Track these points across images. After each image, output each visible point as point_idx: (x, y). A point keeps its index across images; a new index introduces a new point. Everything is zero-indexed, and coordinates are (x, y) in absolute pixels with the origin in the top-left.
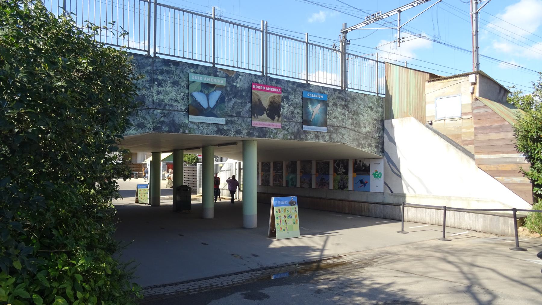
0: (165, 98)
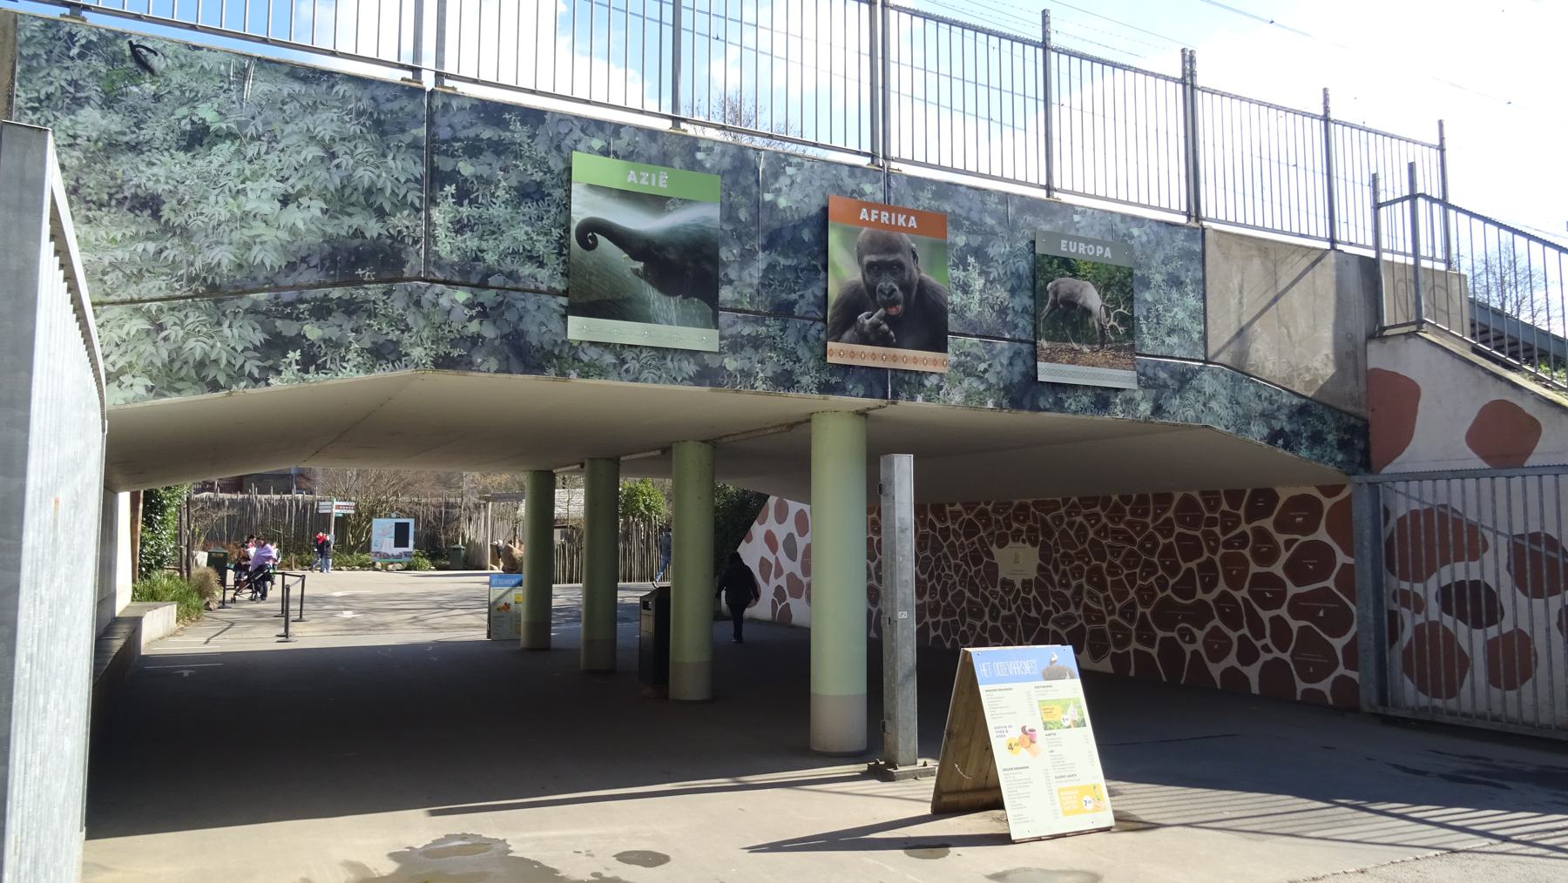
0: (484, 245)
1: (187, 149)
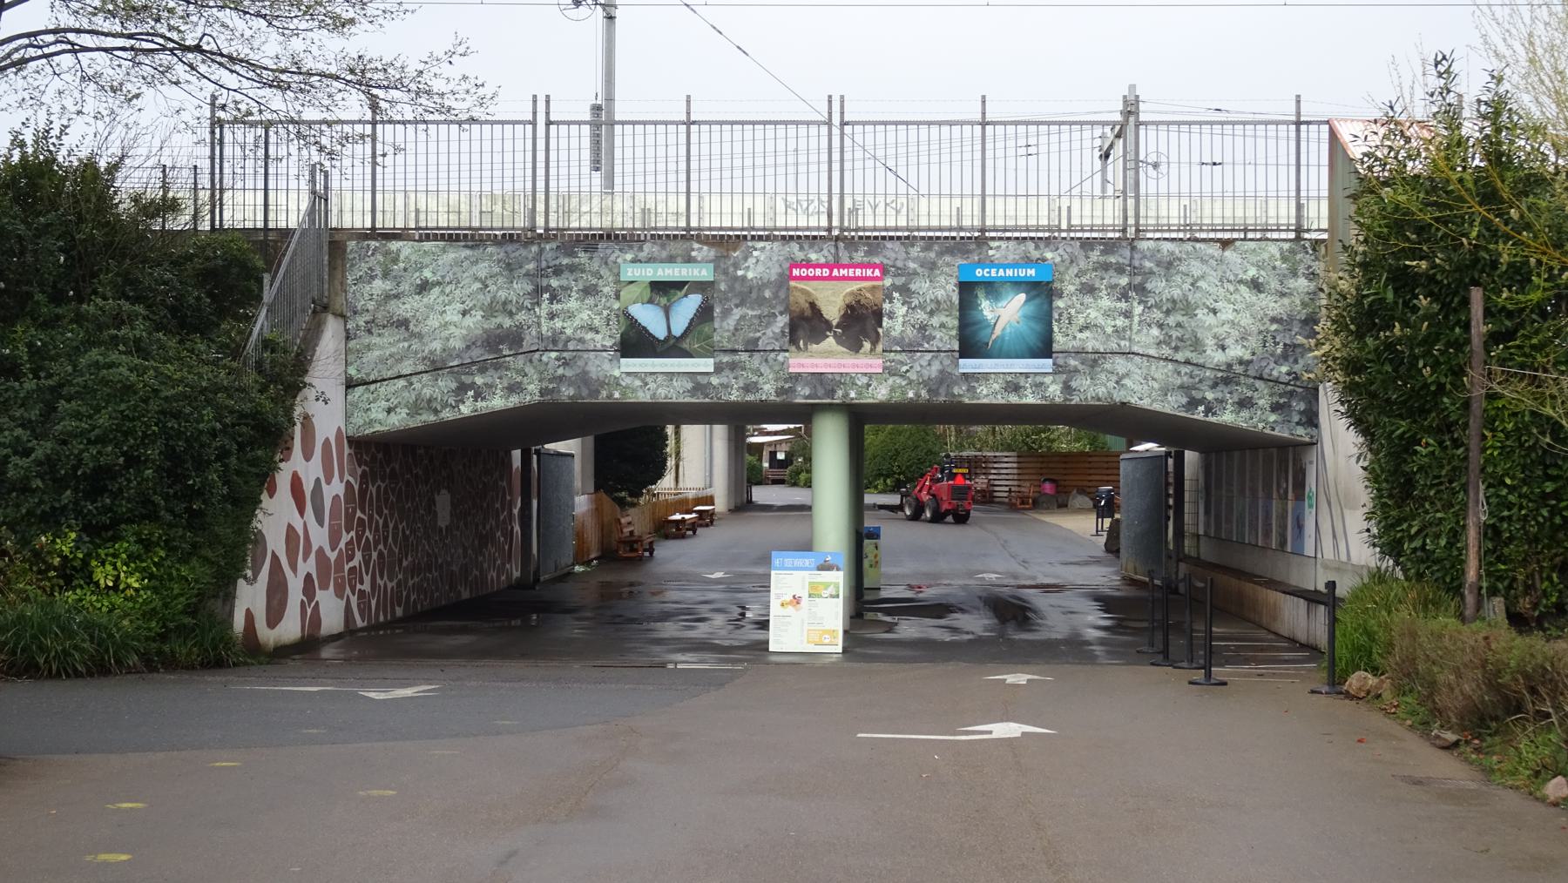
0: (565, 325)
1: (419, 293)
